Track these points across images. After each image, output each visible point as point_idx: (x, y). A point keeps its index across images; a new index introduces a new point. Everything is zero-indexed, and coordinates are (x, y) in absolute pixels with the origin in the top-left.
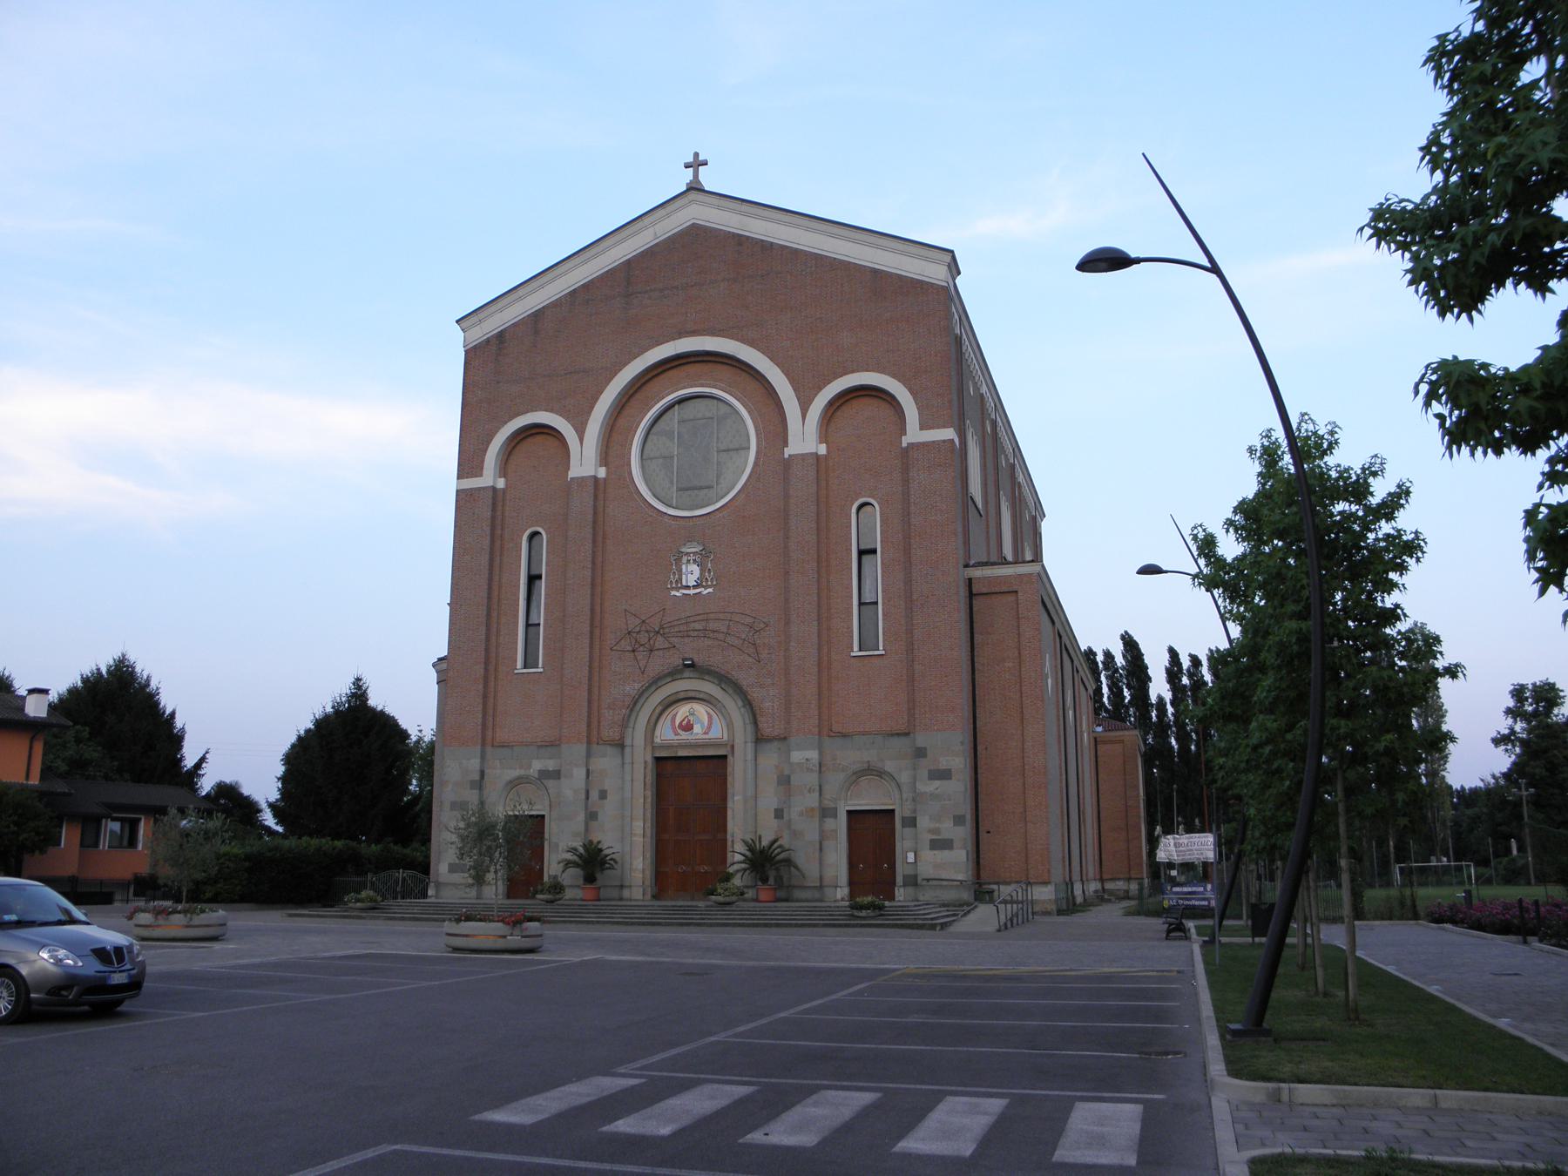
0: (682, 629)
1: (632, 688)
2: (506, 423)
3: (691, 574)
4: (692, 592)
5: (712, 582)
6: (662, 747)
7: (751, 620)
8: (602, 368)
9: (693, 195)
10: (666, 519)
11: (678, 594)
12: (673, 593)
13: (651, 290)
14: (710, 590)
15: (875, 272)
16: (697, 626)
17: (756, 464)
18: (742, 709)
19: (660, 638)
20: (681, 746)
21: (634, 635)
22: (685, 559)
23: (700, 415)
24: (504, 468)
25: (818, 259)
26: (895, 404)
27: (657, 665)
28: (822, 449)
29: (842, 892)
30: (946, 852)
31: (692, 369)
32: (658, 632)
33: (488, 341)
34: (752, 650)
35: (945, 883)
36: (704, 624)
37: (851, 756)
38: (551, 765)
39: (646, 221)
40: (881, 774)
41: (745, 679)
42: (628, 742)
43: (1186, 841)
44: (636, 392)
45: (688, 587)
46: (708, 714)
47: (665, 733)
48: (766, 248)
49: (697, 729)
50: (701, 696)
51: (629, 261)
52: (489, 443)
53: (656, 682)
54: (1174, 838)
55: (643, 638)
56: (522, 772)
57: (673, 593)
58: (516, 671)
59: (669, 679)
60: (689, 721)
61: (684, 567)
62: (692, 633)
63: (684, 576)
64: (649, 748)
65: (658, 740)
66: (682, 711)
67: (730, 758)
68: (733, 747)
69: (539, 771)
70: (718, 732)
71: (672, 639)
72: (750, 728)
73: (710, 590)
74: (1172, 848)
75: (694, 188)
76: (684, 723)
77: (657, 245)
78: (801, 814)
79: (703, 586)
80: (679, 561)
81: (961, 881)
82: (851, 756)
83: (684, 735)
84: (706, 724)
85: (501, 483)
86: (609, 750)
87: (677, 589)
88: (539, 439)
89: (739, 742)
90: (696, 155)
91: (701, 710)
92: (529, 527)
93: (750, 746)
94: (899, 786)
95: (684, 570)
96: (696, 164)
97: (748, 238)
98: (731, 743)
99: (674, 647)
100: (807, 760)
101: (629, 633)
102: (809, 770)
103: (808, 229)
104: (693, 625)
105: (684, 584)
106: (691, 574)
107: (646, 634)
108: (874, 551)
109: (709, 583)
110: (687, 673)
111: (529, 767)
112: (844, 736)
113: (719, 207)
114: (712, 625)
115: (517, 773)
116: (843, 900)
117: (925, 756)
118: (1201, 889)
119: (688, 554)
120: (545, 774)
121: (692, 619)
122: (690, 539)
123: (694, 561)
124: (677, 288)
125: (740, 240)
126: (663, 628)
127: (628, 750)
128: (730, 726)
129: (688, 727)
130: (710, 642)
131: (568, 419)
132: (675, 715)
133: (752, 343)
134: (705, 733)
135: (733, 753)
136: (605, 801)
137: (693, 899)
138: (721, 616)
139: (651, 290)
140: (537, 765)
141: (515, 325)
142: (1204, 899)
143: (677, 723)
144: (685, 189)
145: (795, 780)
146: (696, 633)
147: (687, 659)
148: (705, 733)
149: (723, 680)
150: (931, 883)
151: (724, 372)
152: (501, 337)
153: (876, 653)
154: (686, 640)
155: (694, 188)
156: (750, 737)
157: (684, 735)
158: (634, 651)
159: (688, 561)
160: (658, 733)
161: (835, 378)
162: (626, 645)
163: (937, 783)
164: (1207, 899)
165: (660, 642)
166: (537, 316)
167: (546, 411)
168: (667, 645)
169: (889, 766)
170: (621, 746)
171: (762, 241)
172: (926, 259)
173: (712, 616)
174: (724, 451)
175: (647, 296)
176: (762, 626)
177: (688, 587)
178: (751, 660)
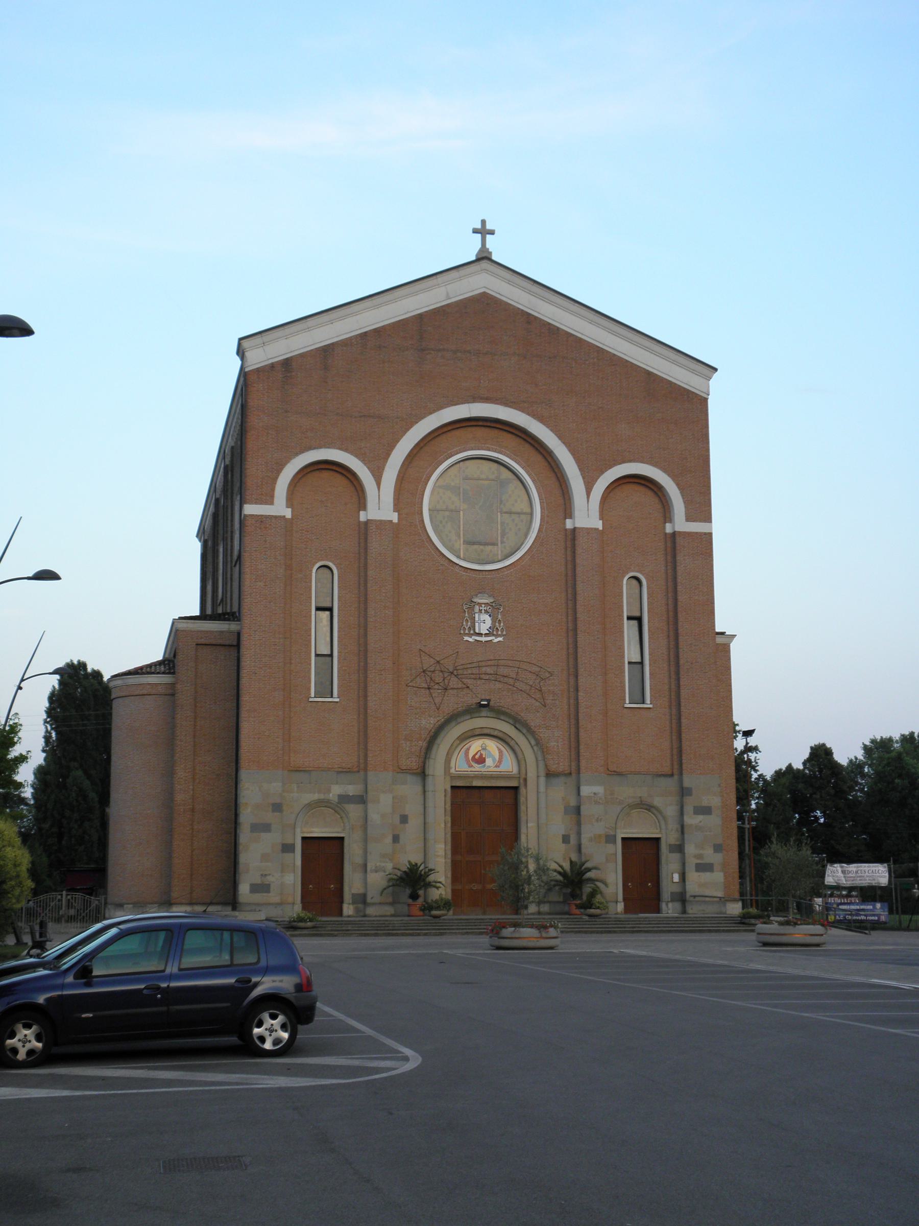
0: (474, 672)
1: (429, 722)
2: (297, 454)
3: (484, 623)
4: (483, 639)
5: (502, 632)
6: (459, 777)
7: (538, 669)
8: (397, 418)
9: (484, 264)
10: (457, 569)
11: (470, 640)
12: (466, 638)
13: (444, 350)
14: (500, 639)
15: (649, 373)
16: (489, 670)
17: (540, 530)
18: (535, 748)
19: (454, 679)
20: (476, 777)
21: (429, 674)
22: (477, 608)
23: (483, 476)
24: (290, 502)
25: (600, 352)
26: (660, 494)
27: (452, 702)
28: (599, 525)
29: (620, 907)
30: (708, 874)
31: (480, 432)
32: (452, 673)
33: (272, 366)
34: (538, 696)
35: (707, 899)
36: (495, 668)
37: (627, 792)
38: (352, 790)
39: (440, 279)
40: (649, 808)
41: (534, 720)
42: (429, 771)
43: (854, 870)
44: (425, 445)
45: (480, 635)
46: (499, 750)
47: (460, 765)
48: (552, 332)
49: (489, 762)
50: (496, 733)
51: (420, 316)
52: (279, 471)
53: (453, 718)
54: (842, 867)
55: (438, 677)
56: (322, 796)
57: (466, 638)
58: (311, 700)
59: (468, 717)
60: (481, 755)
61: (477, 615)
62: (483, 676)
63: (477, 624)
64: (448, 778)
65: (452, 771)
66: (475, 746)
67: (522, 790)
68: (525, 780)
69: (339, 796)
70: (509, 765)
71: (465, 681)
72: (541, 764)
73: (500, 639)
74: (840, 874)
75: (484, 257)
76: (477, 757)
77: (448, 305)
78: (591, 840)
79: (493, 635)
80: (471, 609)
81: (720, 898)
82: (627, 792)
83: (477, 767)
84: (497, 759)
85: (288, 513)
86: (409, 778)
87: (470, 635)
88: (326, 475)
89: (531, 774)
90: (483, 222)
91: (492, 746)
92: (319, 560)
93: (542, 780)
94: (664, 818)
95: (477, 619)
96: (483, 231)
97: (536, 318)
98: (523, 776)
99: (468, 687)
100: (595, 794)
101: (424, 671)
102: (597, 803)
103: (591, 322)
104: (484, 669)
105: (477, 631)
106: (484, 623)
107: (441, 674)
108: (629, 618)
109: (467, 632)
110: (484, 712)
111: (329, 791)
112: (619, 774)
113: (509, 282)
114: (503, 671)
115: (316, 796)
116: (621, 914)
117: (690, 795)
118: (871, 907)
119: (480, 604)
120: (344, 799)
121: (483, 664)
122: (481, 591)
123: (486, 612)
124: (469, 352)
125: (529, 319)
126: (457, 670)
127: (429, 780)
128: (519, 760)
129: (481, 760)
130: (498, 685)
131: (363, 461)
132: (468, 749)
133: (541, 419)
134: (496, 766)
135: (526, 785)
136: (407, 825)
137: (484, 913)
138: (510, 663)
139: (444, 350)
140: (336, 790)
141: (302, 356)
142: (874, 915)
143: (471, 756)
144: (474, 258)
145: (583, 809)
146: (487, 677)
147: (482, 700)
148: (496, 766)
149: (517, 722)
150: (697, 899)
151: (511, 441)
152: (287, 364)
153: (645, 706)
154: (479, 682)
155: (484, 257)
156: (542, 772)
157: (477, 767)
158: (429, 688)
159: (480, 611)
160: (452, 764)
161: (615, 465)
162: (421, 682)
163: (701, 817)
164: (879, 916)
165: (454, 682)
166: (326, 351)
167: (340, 449)
168: (460, 685)
169: (657, 801)
170: (423, 774)
171: (549, 324)
172: (693, 371)
173: (502, 662)
174: (506, 513)
175: (440, 354)
176: (547, 675)
177: (480, 635)
178: (538, 704)
